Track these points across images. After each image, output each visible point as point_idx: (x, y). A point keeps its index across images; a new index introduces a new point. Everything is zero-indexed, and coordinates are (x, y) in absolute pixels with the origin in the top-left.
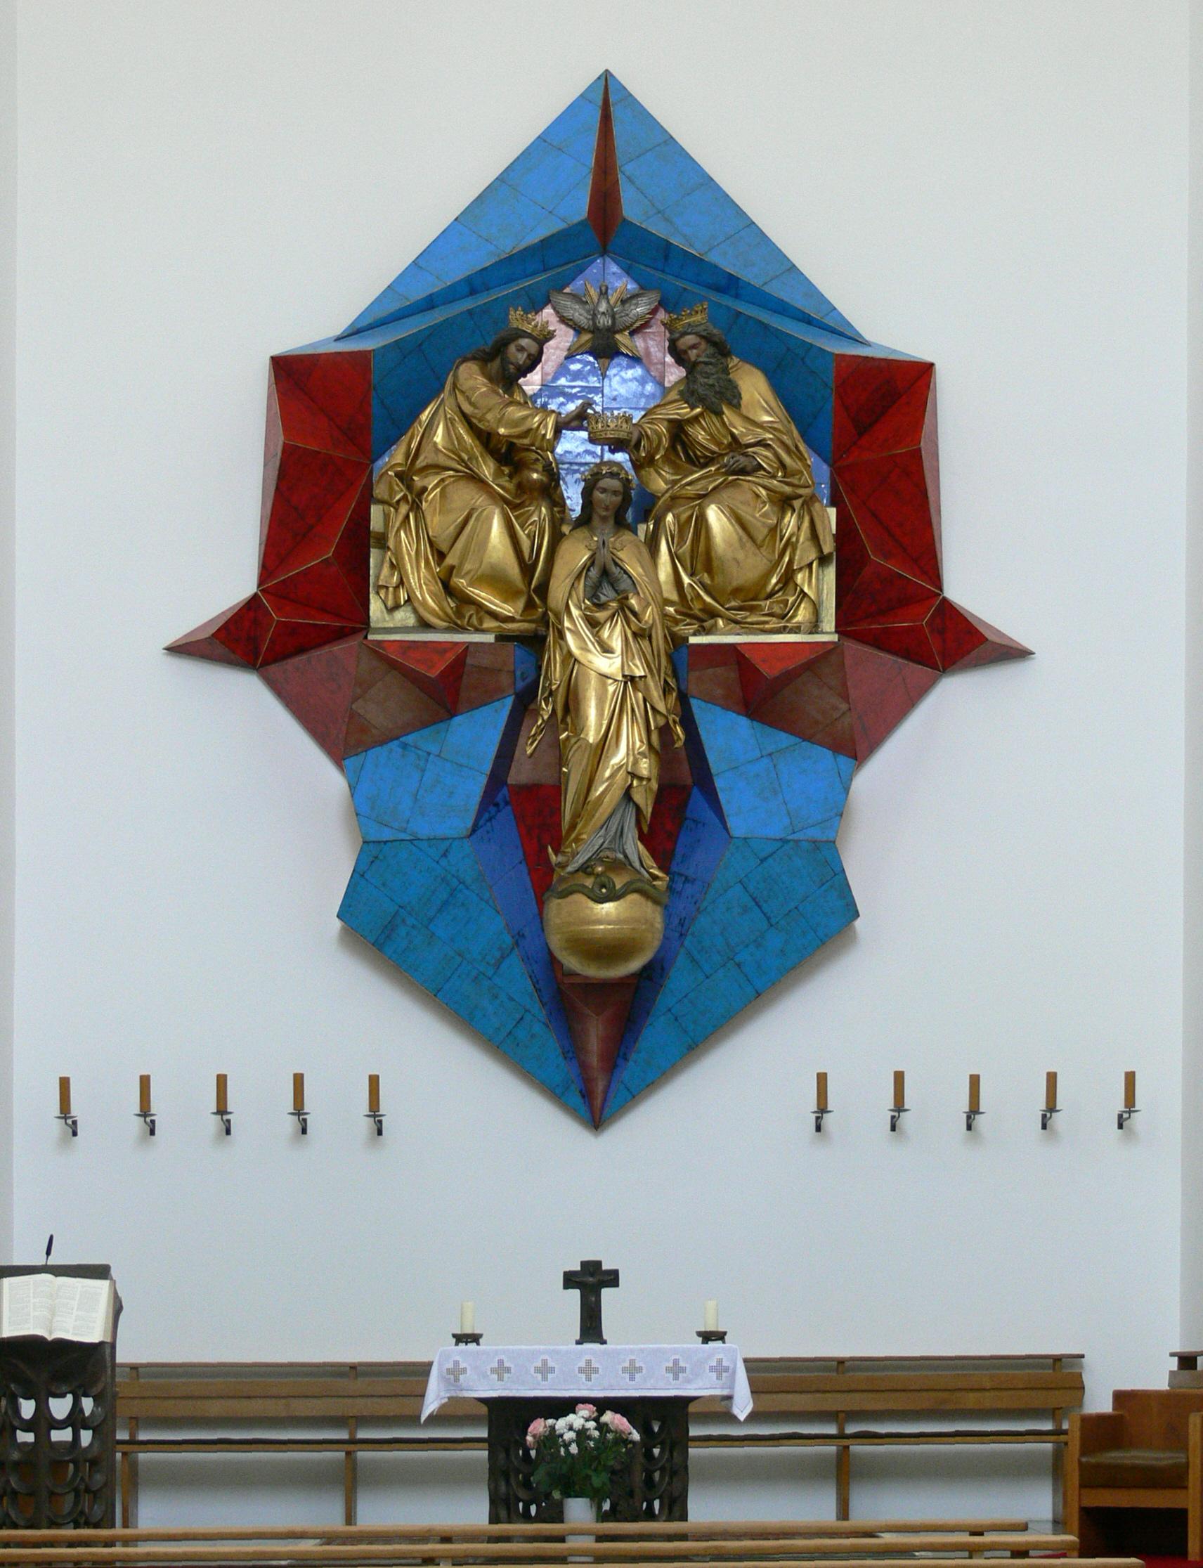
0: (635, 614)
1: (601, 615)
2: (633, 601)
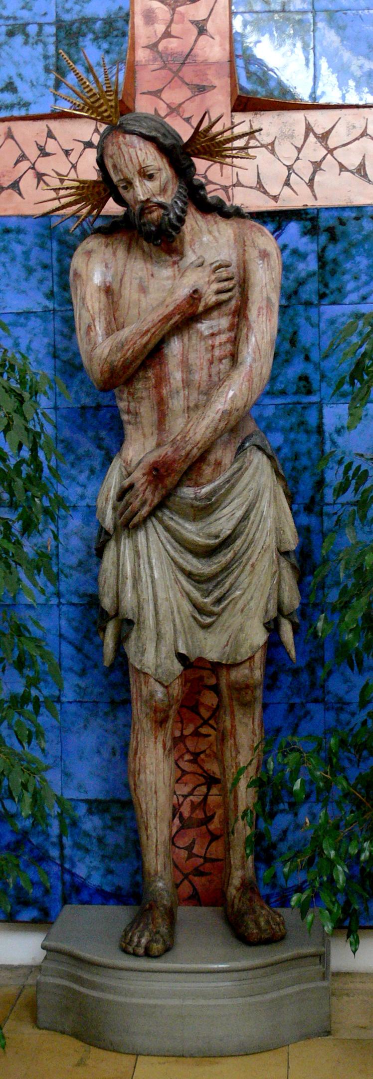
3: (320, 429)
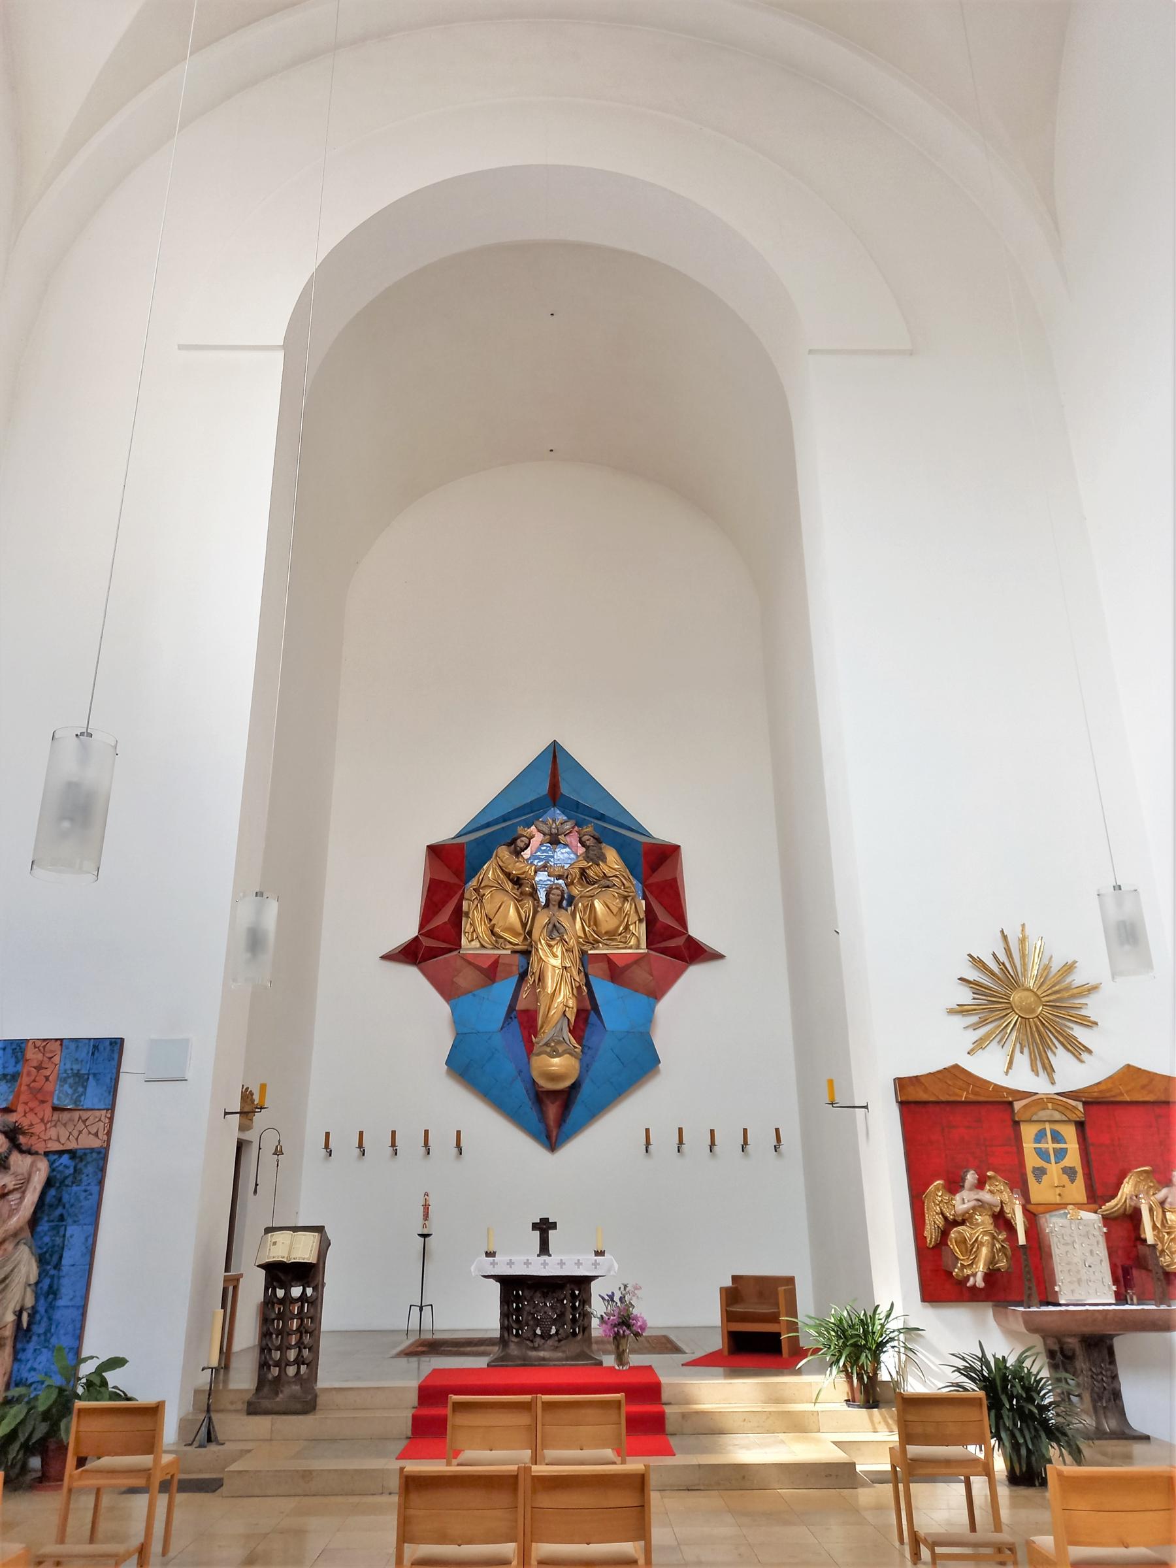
0: (566, 942)
1: (552, 943)
2: (565, 937)
3: (64, 1236)
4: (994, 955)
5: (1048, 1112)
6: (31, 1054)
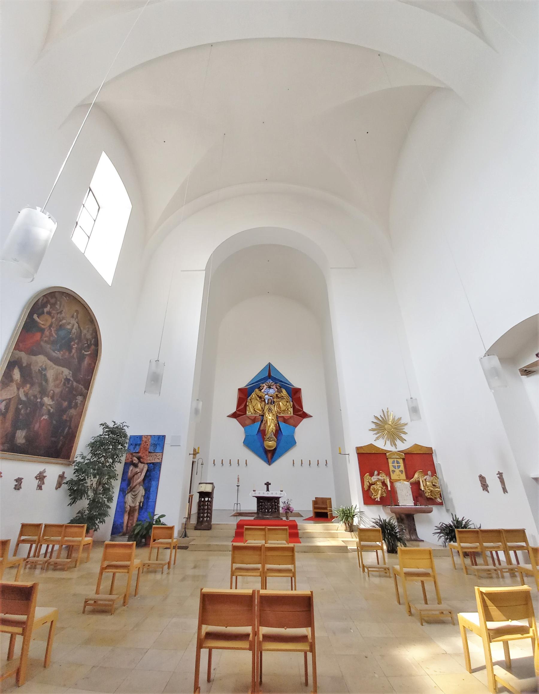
1: (269, 413)
4: (380, 415)
5: (395, 456)
6: (144, 439)
